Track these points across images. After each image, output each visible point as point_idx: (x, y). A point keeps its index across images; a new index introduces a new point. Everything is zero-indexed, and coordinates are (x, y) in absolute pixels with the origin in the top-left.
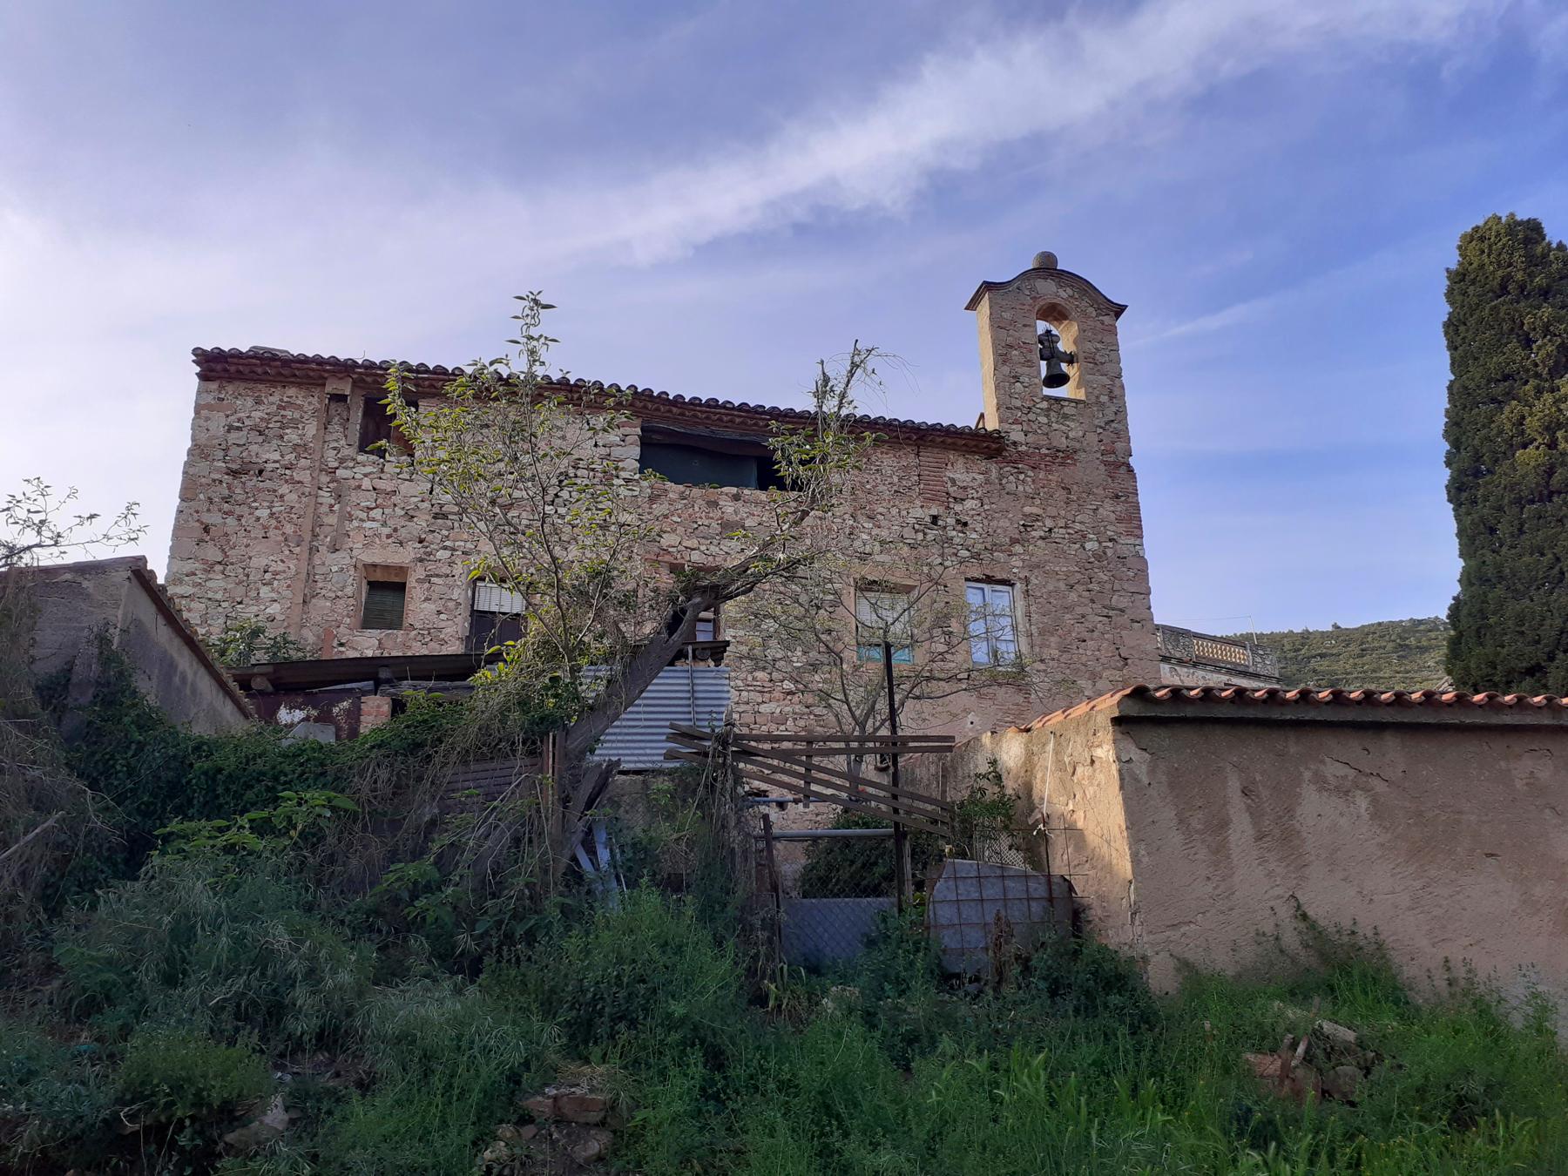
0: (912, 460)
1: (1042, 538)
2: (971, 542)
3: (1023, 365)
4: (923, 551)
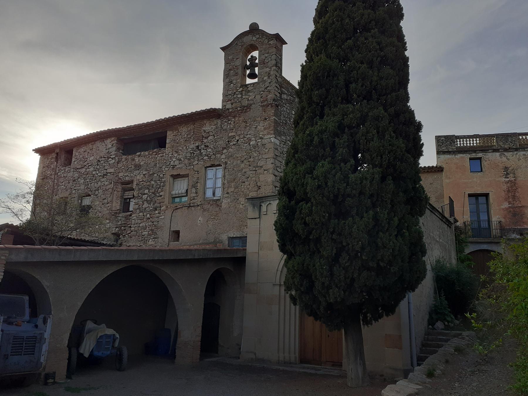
0: (192, 127)
1: (234, 144)
2: (208, 153)
3: (234, 76)
4: (192, 160)
